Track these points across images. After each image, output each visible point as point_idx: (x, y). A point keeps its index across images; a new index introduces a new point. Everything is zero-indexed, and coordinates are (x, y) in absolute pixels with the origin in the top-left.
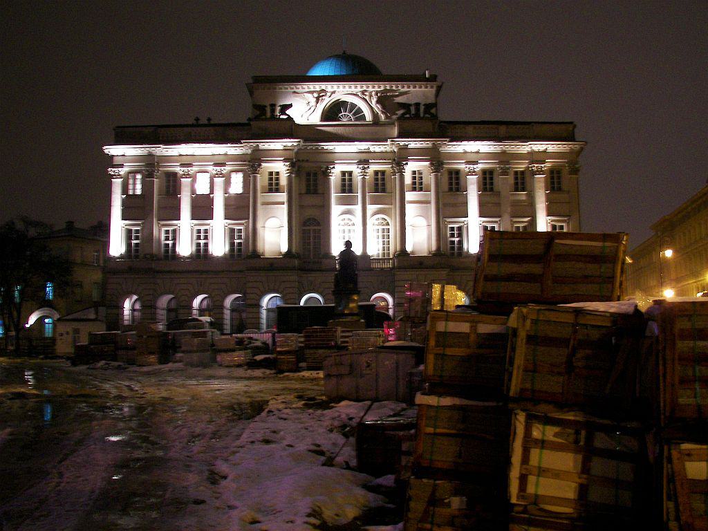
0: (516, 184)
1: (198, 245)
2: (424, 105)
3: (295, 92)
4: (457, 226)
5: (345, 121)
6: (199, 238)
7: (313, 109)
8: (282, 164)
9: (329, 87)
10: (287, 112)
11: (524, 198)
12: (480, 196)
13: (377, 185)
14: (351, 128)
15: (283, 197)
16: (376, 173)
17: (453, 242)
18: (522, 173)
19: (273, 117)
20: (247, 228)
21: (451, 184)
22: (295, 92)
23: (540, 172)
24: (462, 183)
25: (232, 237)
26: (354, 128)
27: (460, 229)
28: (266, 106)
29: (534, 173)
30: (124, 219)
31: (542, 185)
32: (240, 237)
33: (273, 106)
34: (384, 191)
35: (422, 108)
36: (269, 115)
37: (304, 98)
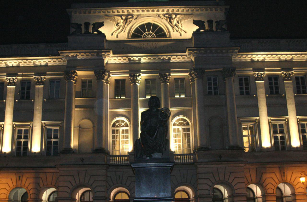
0: (298, 88)
1: (19, 143)
2: (216, 22)
3: (106, 15)
5: (149, 38)
6: (20, 137)
7: (121, 28)
9: (135, 10)
10: (100, 29)
14: (154, 43)
18: (302, 78)
19: (87, 32)
20: (61, 128)
21: (241, 88)
22: (106, 15)
25: (49, 137)
26: (156, 43)
28: (81, 25)
32: (56, 137)
33: (87, 25)
35: (214, 25)
36: (83, 32)
37: (114, 20)
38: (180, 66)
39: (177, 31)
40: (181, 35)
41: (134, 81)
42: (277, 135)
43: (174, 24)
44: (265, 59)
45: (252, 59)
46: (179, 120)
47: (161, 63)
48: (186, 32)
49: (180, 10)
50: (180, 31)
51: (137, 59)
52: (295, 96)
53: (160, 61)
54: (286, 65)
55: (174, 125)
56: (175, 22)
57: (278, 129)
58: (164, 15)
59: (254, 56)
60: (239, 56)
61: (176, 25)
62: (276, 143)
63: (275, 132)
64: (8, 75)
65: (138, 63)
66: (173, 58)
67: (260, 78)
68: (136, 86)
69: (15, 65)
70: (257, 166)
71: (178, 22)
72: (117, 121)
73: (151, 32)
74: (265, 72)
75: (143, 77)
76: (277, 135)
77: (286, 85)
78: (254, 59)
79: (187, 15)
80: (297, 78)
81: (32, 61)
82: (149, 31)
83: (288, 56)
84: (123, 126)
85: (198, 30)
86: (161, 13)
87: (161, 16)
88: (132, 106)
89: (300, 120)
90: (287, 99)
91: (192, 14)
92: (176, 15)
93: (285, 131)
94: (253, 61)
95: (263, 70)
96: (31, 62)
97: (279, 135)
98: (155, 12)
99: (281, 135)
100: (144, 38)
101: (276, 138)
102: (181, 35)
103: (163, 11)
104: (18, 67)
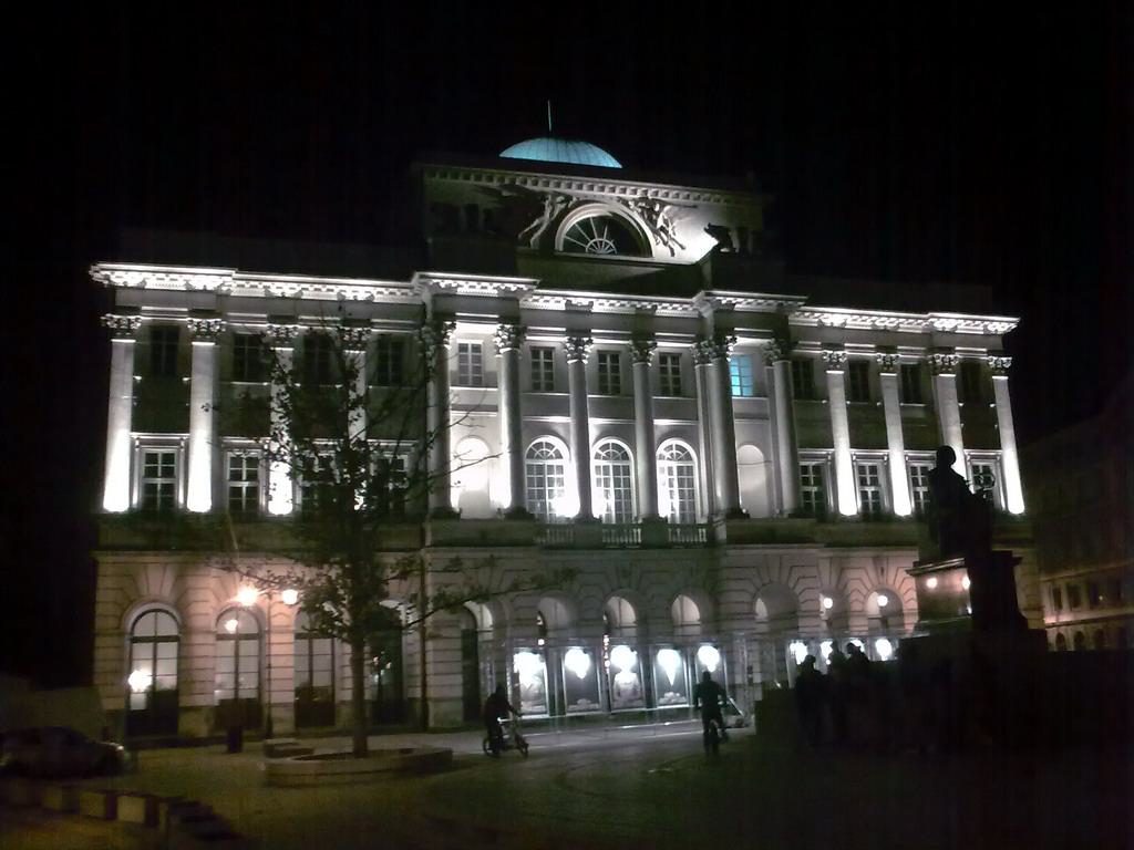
4: (814, 463)
5: (603, 253)
8: (493, 328)
11: (920, 415)
12: (849, 408)
13: (664, 380)
15: (501, 395)
16: (602, 355)
17: (807, 495)
23: (946, 368)
24: (817, 382)
27: (817, 469)
29: (936, 370)
30: (134, 429)
31: (953, 391)
34: (677, 392)
38: (674, 325)
39: (665, 244)
40: (673, 254)
41: (579, 355)
42: (867, 489)
43: (658, 226)
44: (845, 324)
45: (820, 321)
46: (670, 447)
47: (636, 315)
48: (684, 245)
49: (671, 195)
50: (670, 243)
51: (585, 302)
52: (901, 407)
53: (633, 311)
54: (886, 340)
55: (662, 457)
56: (660, 223)
57: (868, 476)
58: (636, 202)
59: (826, 315)
60: (797, 313)
61: (662, 229)
62: (865, 505)
63: (863, 482)
64: (272, 319)
65: (586, 311)
66: (663, 308)
67: (834, 365)
68: (579, 365)
69: (289, 293)
70: (831, 554)
71: (665, 221)
72: (539, 445)
73: (604, 240)
74: (846, 352)
75: (598, 343)
76: (867, 489)
77: (884, 384)
78: (824, 321)
79: (686, 206)
80: (904, 369)
81: (337, 289)
82: (601, 235)
83: (892, 319)
84: (551, 458)
85: (716, 250)
86: (628, 195)
87: (630, 203)
88: (572, 413)
89: (911, 458)
90: (886, 412)
91: (695, 207)
92: (663, 204)
93: (882, 480)
94: (822, 326)
95: (840, 347)
96: (332, 290)
97: (870, 490)
98: (617, 194)
99: (873, 489)
100: (590, 252)
101: (864, 495)
102: (673, 254)
103: (635, 192)
104: (297, 299)
